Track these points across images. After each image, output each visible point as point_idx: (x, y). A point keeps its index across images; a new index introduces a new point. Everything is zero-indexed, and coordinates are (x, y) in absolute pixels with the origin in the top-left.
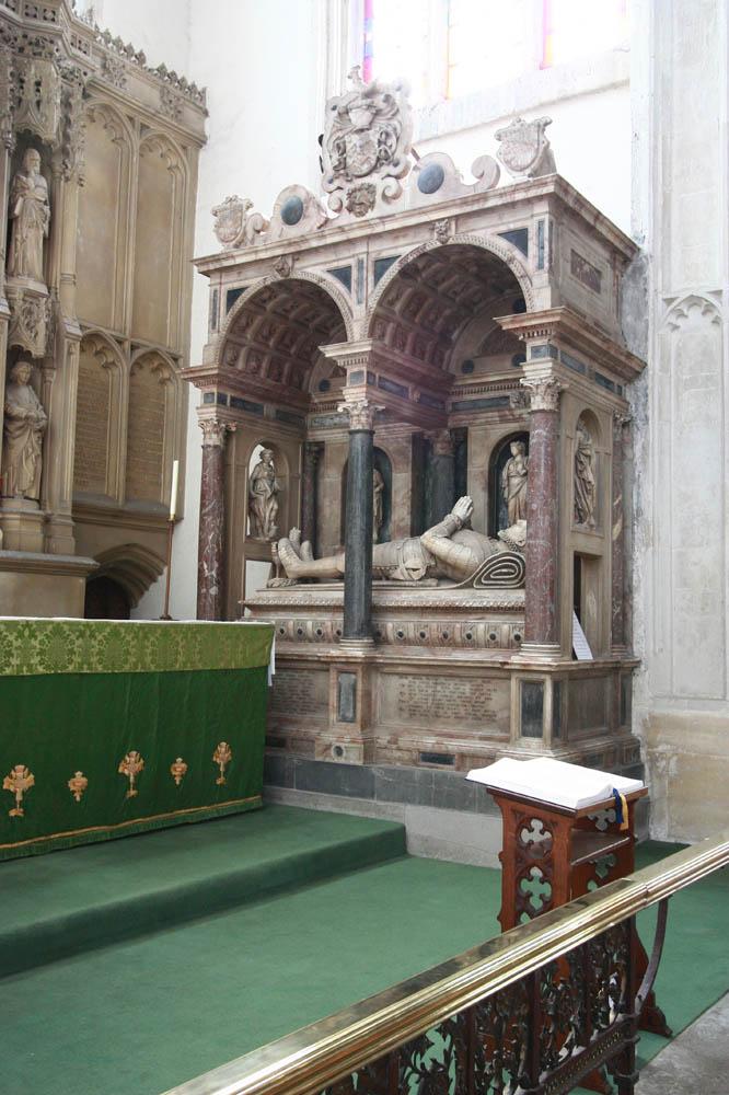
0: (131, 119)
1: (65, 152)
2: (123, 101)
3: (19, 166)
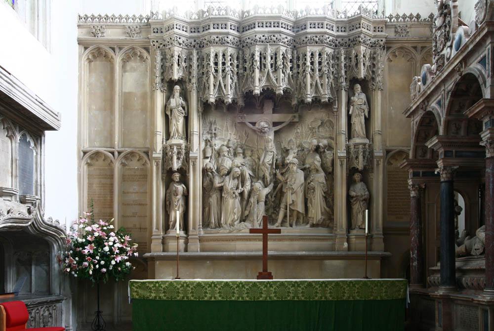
0: (415, 48)
1: (373, 79)
2: (408, 42)
3: (351, 91)
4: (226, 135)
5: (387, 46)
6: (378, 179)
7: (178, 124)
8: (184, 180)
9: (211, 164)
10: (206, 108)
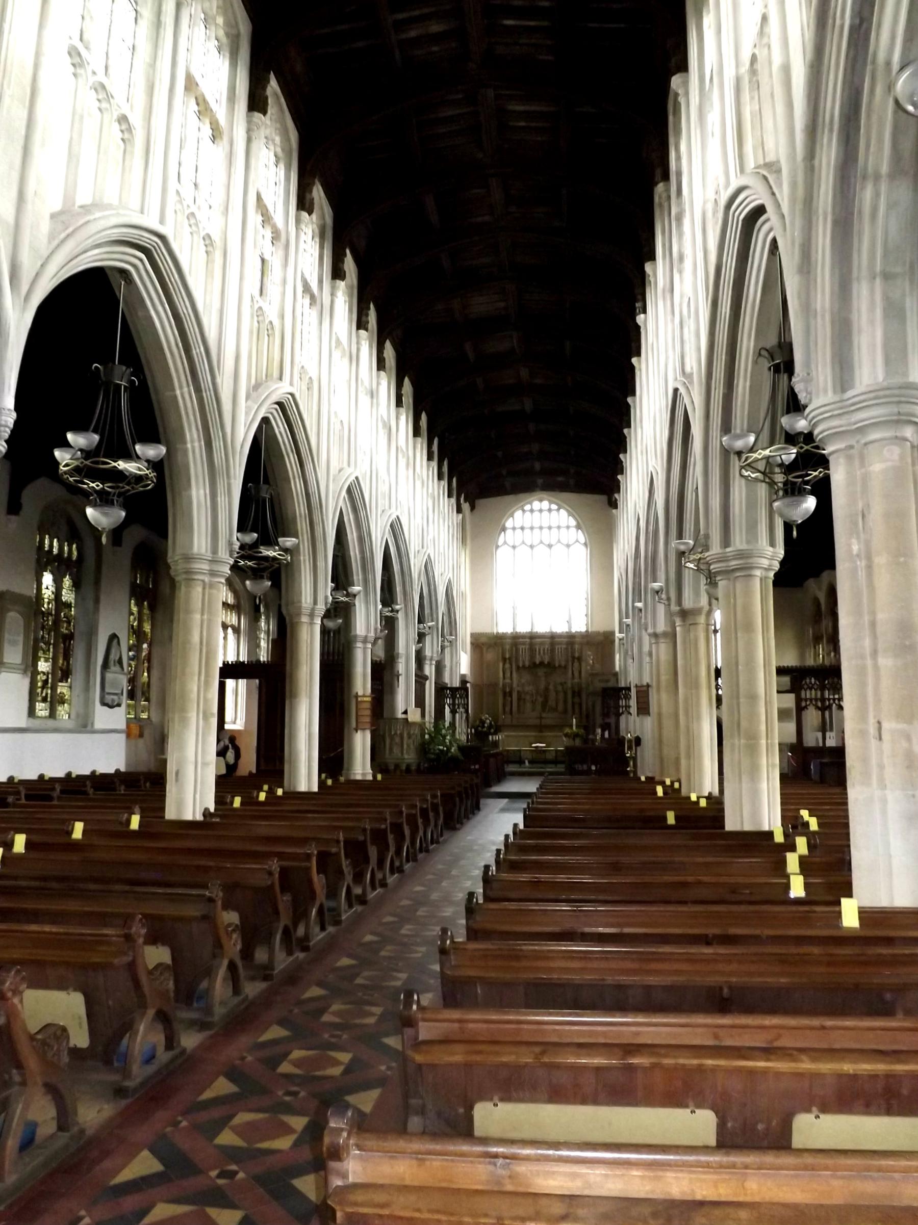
4: (526, 677)
5: (588, 643)
6: (584, 696)
7: (508, 674)
8: (511, 696)
9: (520, 689)
10: (518, 668)
